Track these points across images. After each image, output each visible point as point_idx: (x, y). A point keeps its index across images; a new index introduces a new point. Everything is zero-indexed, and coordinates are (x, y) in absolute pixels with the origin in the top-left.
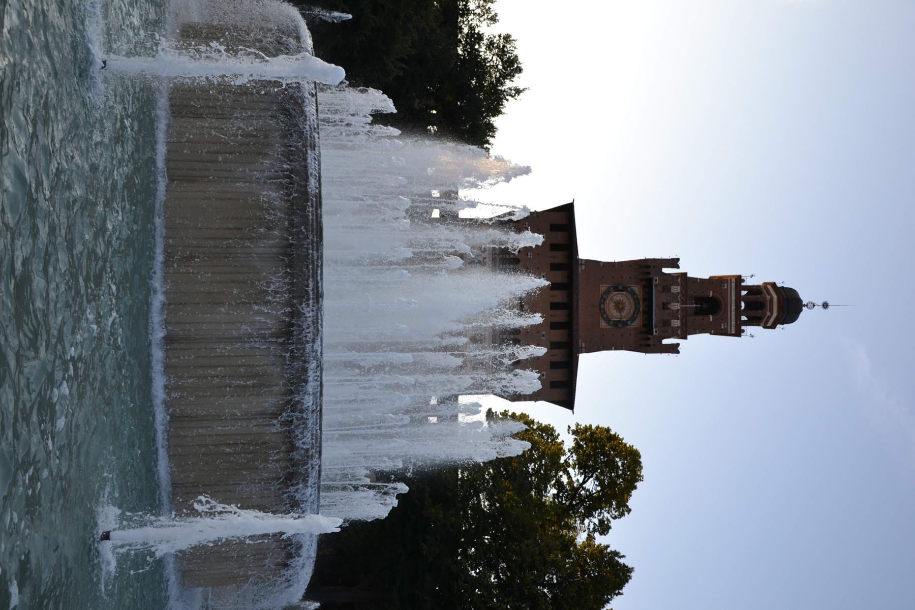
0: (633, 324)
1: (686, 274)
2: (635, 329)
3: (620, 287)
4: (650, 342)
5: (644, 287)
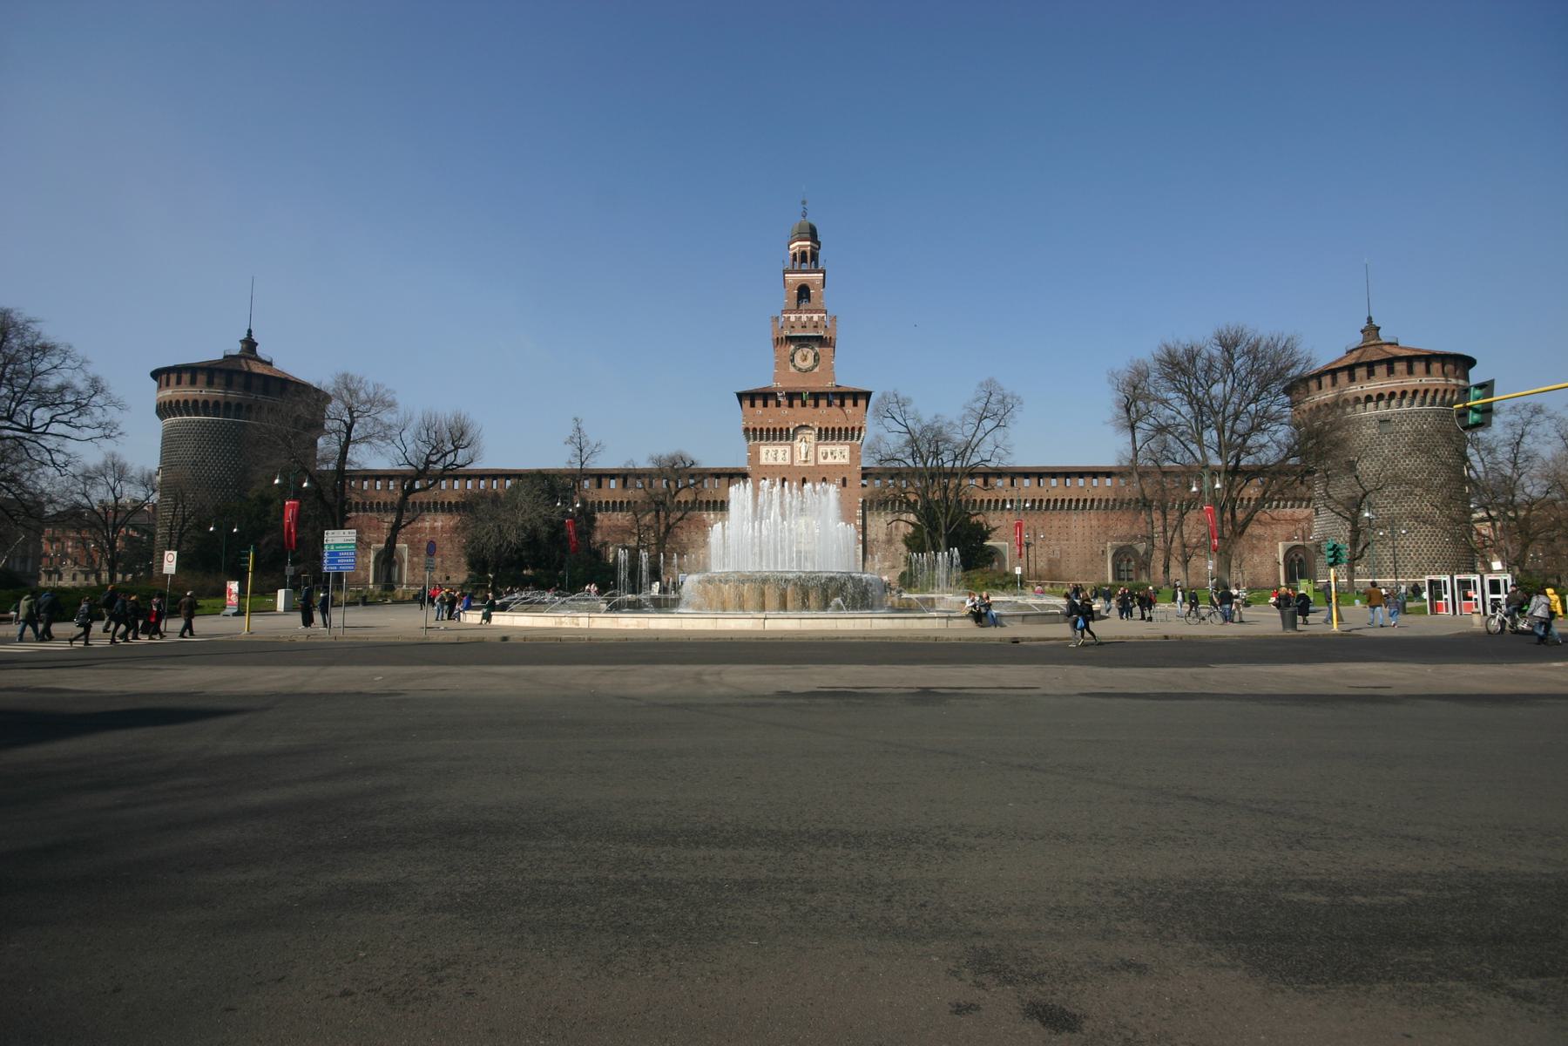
5: (791, 341)
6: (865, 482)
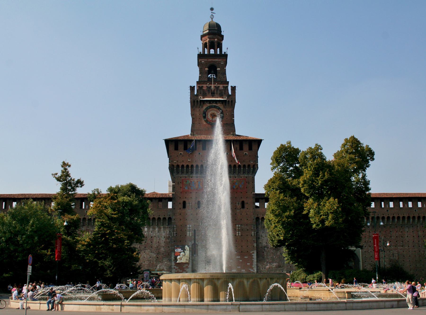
1: (197, 82)
3: (204, 115)
4: (230, 101)
5: (204, 103)
6: (257, 204)
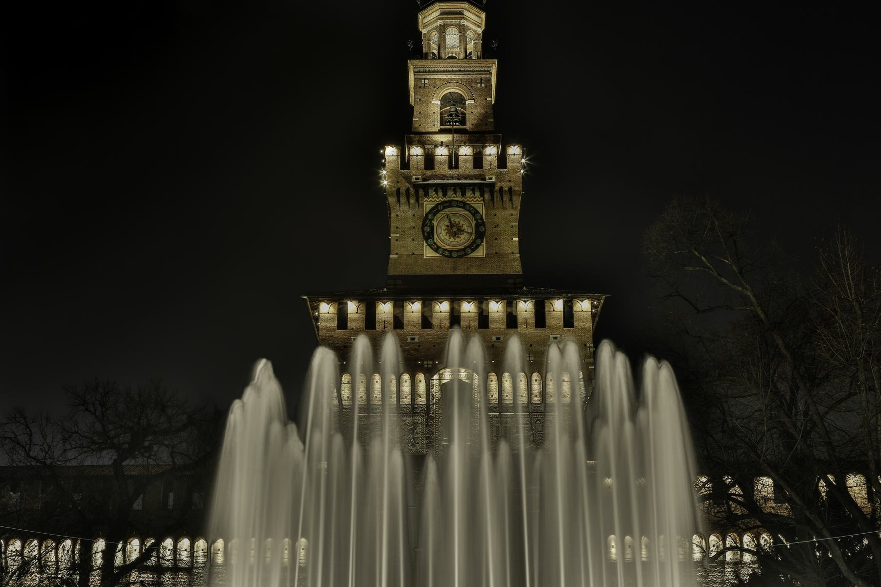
0: (480, 210)
2: (487, 210)
3: (427, 229)
4: (505, 189)
5: (426, 195)
